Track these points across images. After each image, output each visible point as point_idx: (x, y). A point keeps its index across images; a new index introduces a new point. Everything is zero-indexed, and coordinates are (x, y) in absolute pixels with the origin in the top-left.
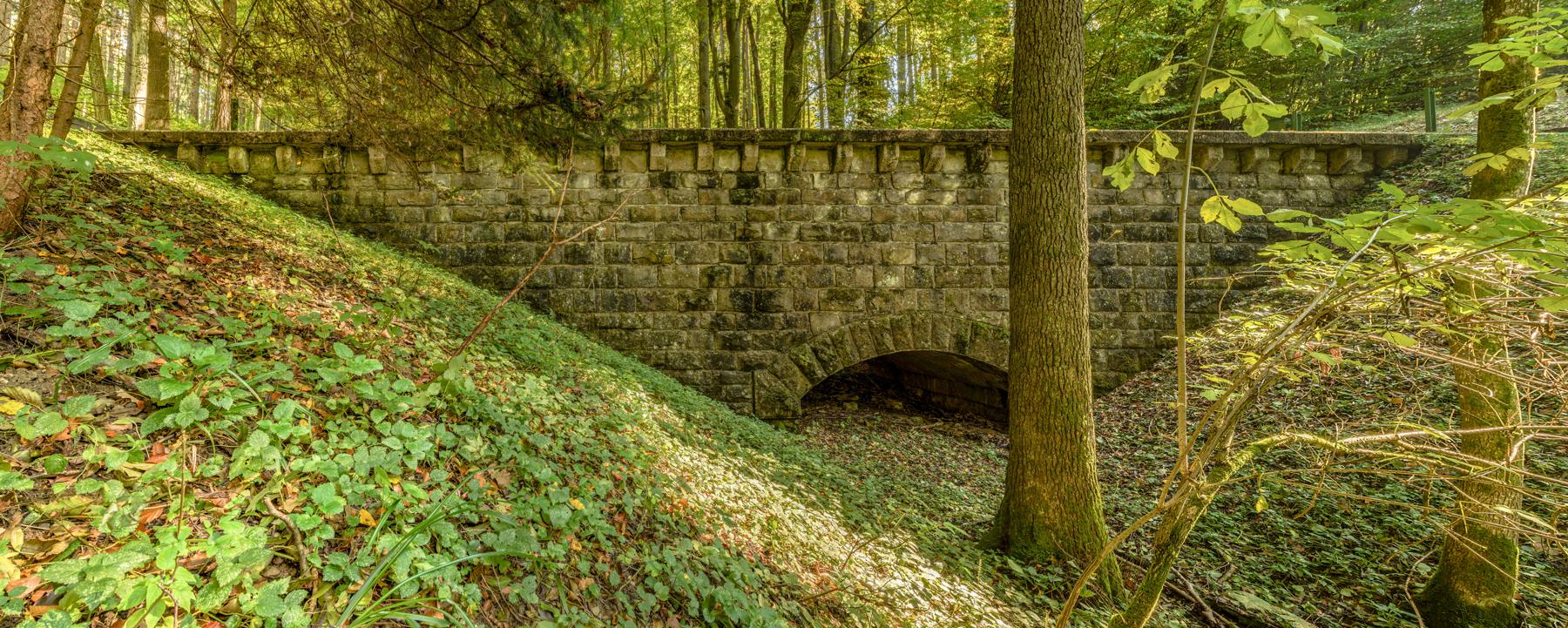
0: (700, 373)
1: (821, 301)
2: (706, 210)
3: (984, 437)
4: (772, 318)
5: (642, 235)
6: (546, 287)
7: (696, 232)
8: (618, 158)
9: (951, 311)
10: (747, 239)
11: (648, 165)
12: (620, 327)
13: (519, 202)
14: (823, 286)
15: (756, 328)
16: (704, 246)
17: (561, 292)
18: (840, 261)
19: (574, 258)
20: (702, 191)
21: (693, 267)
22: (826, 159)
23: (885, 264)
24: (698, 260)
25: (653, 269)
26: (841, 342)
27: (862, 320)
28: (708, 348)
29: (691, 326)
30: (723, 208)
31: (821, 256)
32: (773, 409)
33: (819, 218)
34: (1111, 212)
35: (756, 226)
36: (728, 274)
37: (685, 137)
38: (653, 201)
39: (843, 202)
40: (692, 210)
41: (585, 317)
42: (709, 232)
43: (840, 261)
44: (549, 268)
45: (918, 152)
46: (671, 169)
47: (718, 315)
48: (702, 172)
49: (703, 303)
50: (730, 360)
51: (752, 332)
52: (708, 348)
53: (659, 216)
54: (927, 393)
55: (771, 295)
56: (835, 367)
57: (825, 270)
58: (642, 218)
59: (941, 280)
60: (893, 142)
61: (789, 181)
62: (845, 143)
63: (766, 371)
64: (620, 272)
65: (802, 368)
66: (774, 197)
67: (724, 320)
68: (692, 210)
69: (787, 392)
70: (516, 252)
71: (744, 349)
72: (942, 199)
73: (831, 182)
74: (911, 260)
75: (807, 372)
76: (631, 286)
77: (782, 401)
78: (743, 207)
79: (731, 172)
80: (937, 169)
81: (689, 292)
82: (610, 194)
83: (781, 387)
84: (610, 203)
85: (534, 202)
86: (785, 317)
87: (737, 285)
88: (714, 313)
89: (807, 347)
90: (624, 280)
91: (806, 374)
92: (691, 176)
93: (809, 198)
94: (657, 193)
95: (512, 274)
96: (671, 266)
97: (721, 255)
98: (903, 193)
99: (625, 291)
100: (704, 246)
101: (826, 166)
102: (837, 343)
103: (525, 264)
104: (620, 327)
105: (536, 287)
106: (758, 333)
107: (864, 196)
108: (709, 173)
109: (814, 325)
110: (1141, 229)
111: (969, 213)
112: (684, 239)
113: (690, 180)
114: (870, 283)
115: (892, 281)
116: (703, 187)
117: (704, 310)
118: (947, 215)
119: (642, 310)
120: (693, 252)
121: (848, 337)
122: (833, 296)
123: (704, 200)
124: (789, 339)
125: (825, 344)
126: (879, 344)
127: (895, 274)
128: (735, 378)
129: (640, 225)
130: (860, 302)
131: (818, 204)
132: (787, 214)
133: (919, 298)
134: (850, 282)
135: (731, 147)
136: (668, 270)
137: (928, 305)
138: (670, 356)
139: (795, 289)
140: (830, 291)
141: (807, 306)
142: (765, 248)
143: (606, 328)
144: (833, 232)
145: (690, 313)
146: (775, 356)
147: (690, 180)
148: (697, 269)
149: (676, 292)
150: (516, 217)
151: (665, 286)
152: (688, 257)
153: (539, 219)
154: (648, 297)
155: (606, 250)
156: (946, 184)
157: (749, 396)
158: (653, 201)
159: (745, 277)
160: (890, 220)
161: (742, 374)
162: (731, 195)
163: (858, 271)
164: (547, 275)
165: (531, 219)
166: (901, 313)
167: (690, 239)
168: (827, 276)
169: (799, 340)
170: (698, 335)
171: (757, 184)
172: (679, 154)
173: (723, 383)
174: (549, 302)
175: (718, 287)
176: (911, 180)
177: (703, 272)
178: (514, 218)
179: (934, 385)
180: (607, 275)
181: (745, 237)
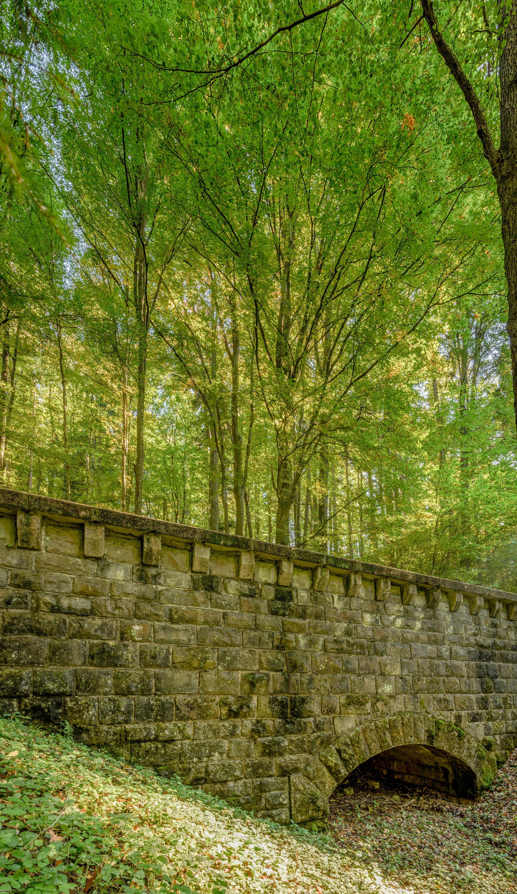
0: (240, 783)
1: (342, 705)
2: (247, 618)
3: (444, 809)
4: (305, 723)
5: (183, 637)
6: (63, 694)
7: (238, 639)
8: (158, 552)
9: (423, 711)
10: (283, 648)
11: (191, 565)
12: (156, 739)
13: (27, 585)
14: (342, 692)
15: (291, 733)
16: (245, 653)
17: (82, 700)
18: (353, 671)
19: (102, 659)
20: (244, 599)
21: (235, 674)
22: (341, 583)
23: (382, 674)
24: (240, 666)
25: (195, 675)
26: (358, 742)
27: (371, 722)
28: (248, 756)
29: (233, 734)
30: (262, 617)
31: (340, 665)
32: (307, 811)
33: (338, 633)
34: (495, 643)
35: (291, 637)
36: (268, 681)
37: (229, 543)
38: (195, 602)
39: (355, 622)
40: (234, 616)
41: (113, 729)
42: (249, 639)
43: (353, 671)
44: (67, 671)
45: (399, 588)
46: (214, 573)
47: (258, 722)
48: (244, 581)
49: (245, 710)
50: (268, 767)
51: (288, 736)
52: (248, 756)
53: (201, 619)
54: (391, 772)
55: (303, 701)
56: (354, 764)
57: (344, 679)
58: (182, 620)
59: (416, 688)
60: (387, 577)
61: (316, 598)
62: (357, 572)
63: (300, 774)
64: (157, 678)
65: (329, 768)
66: (304, 611)
67: (264, 726)
68: (234, 616)
69: (318, 793)
70: (19, 648)
71: (281, 754)
72: (415, 625)
73: (346, 604)
74: (398, 672)
75: (333, 772)
76: (170, 693)
77: (314, 802)
78: (279, 618)
79: (269, 584)
80: (411, 603)
81: (231, 699)
82: (149, 590)
83: (314, 789)
84: (148, 600)
85: (49, 588)
86: (315, 721)
87: (275, 692)
88: (254, 720)
89: (333, 748)
90: (162, 686)
91: (332, 774)
92: (233, 583)
93: (331, 616)
94: (200, 595)
95: (11, 676)
96: (213, 672)
97: (260, 662)
98: (392, 618)
99: (162, 698)
100: (245, 653)
101: (342, 590)
102: (354, 743)
103: (32, 664)
104: (156, 739)
105: (47, 694)
106: (294, 737)
107: (368, 618)
108: (250, 582)
109: (337, 728)
110: (508, 655)
111: (429, 638)
112: (226, 644)
113: (233, 587)
114: (373, 690)
115: (388, 689)
116: (245, 595)
117: (245, 717)
118: (417, 639)
119: (181, 718)
120: (234, 658)
121: (362, 737)
122: (351, 702)
123: (245, 608)
124: (319, 741)
125: (346, 744)
126: (383, 741)
127: (389, 683)
128: (273, 784)
129: (181, 627)
130: (368, 706)
131: (338, 621)
132: (315, 628)
133: (405, 702)
134: (361, 689)
135: (270, 561)
136: (210, 676)
137: (410, 708)
138: (211, 768)
139: (322, 696)
140: (348, 697)
141: (331, 710)
142: (298, 657)
143: (139, 741)
144: (348, 646)
145: (232, 721)
146: (307, 759)
147: (233, 587)
148: (239, 675)
149: (218, 699)
150: (22, 603)
151: (207, 693)
152: (230, 663)
153: (55, 609)
154: (188, 705)
155: (142, 652)
156: (417, 614)
157: (286, 802)
158: (195, 602)
159: (282, 684)
160: (384, 639)
161: (280, 779)
162: (269, 606)
163: (366, 680)
164: (64, 678)
165: (43, 607)
166: (394, 715)
167: (233, 645)
168: (344, 683)
169: (326, 742)
170: (239, 744)
171: (291, 599)
172: (222, 559)
173: (262, 791)
174: (65, 713)
175: (258, 694)
176: (396, 609)
177: (244, 678)
178: (18, 605)
179: (395, 766)
180: (142, 680)
181: (280, 647)
